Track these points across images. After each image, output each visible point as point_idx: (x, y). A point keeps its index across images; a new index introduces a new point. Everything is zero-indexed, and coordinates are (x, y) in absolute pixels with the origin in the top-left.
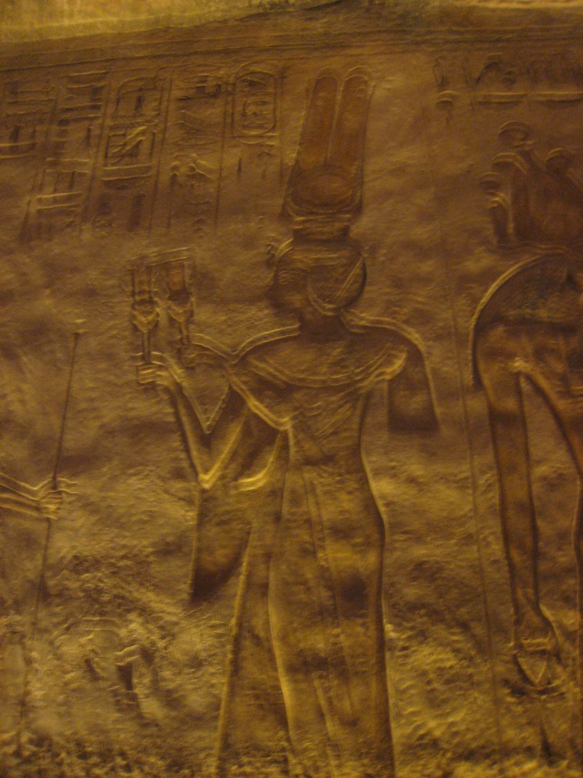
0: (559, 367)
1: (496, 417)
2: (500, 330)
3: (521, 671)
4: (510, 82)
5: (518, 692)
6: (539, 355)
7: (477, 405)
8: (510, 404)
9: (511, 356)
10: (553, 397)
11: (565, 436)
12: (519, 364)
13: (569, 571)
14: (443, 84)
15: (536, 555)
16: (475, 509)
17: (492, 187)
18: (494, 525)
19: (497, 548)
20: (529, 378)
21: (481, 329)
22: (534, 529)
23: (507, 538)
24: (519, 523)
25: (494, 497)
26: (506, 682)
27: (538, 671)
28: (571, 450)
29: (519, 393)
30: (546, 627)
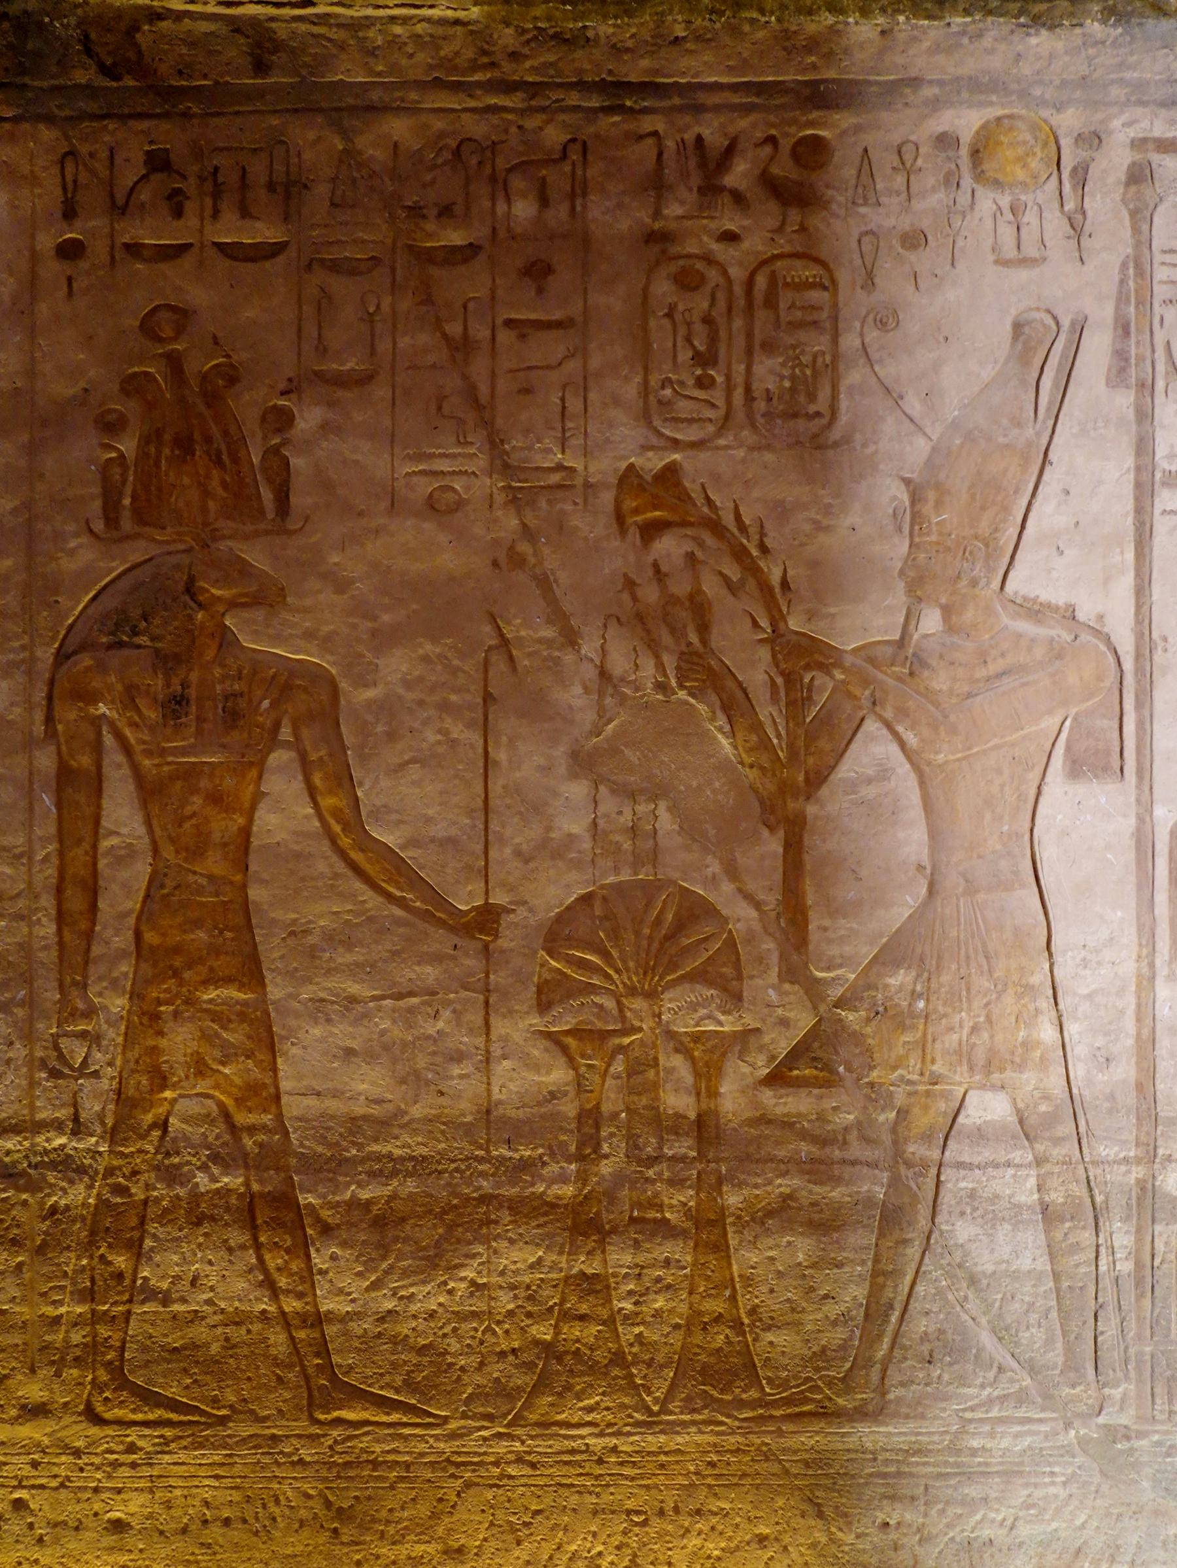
0: (152, 715)
1: (65, 775)
2: (86, 660)
3: (61, 1057)
4: (176, 204)
5: (55, 1074)
6: (130, 697)
7: (46, 761)
8: (85, 761)
9: (92, 698)
10: (138, 748)
11: (144, 804)
12: (102, 708)
13: (122, 955)
14: (70, 213)
15: (89, 936)
16: (30, 884)
17: (111, 426)
18: (47, 901)
19: (47, 929)
20: (112, 724)
21: (62, 657)
22: (93, 908)
23: (61, 918)
24: (76, 902)
25: (51, 871)
26: (43, 1063)
27: (77, 1052)
28: (148, 823)
29: (97, 748)
30: (90, 1012)
